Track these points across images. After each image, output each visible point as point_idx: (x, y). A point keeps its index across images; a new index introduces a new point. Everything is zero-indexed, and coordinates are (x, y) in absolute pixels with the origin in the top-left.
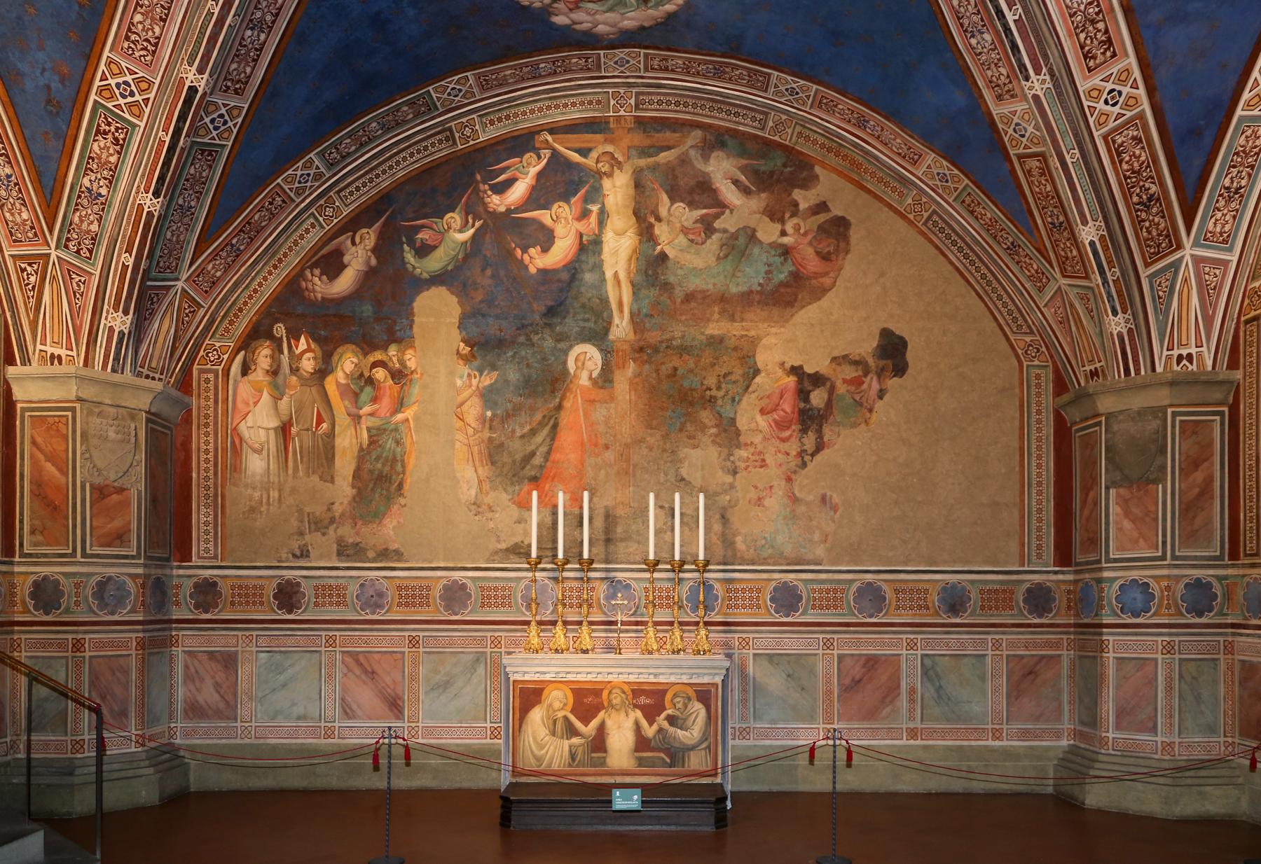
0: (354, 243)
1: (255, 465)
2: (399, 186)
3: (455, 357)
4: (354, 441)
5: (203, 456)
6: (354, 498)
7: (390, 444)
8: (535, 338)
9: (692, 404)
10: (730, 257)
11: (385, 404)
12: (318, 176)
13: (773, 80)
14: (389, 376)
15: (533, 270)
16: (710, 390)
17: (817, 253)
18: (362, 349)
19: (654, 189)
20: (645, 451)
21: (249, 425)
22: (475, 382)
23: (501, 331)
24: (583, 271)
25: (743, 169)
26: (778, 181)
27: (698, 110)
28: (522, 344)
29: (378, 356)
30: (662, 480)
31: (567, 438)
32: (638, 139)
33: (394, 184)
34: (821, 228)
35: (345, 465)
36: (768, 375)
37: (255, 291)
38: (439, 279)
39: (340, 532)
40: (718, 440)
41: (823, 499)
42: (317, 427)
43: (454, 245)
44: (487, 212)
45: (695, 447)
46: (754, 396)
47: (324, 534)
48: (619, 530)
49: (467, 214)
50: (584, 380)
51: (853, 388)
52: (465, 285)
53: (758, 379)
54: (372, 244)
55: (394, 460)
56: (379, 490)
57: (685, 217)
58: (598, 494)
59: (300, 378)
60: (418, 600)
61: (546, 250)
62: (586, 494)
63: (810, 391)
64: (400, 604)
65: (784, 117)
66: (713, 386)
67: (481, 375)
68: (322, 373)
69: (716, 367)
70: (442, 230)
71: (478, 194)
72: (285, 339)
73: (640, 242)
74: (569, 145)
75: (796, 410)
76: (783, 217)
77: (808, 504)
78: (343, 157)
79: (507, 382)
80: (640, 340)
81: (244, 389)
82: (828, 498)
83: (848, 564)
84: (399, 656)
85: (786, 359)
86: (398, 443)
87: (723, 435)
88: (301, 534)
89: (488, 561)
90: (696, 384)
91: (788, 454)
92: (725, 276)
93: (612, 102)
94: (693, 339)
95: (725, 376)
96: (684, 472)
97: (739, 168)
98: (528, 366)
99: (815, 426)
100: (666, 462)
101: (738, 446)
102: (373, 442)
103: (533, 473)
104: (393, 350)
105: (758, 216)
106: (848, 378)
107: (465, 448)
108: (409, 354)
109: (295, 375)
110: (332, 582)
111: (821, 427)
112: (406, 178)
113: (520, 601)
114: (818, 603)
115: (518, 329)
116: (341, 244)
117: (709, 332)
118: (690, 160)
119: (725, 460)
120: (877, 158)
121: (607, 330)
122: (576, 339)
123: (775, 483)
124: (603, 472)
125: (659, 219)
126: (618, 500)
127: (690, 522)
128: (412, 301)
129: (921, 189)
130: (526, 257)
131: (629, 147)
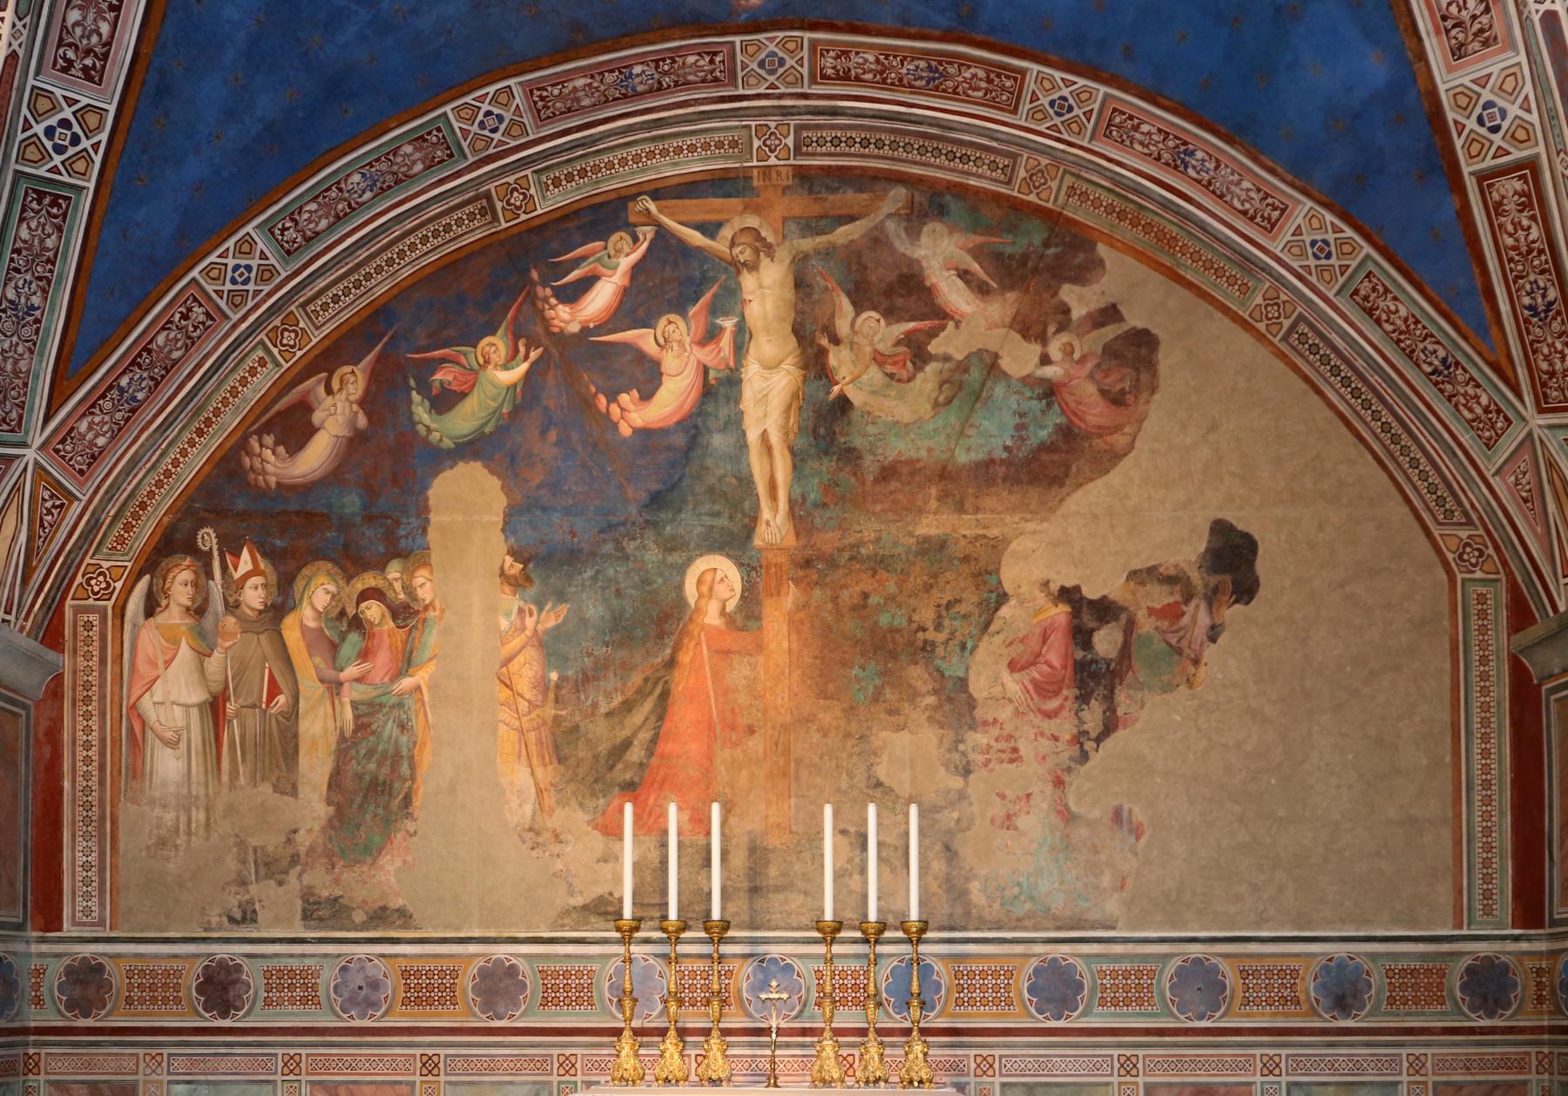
0: (329, 391)
1: (167, 766)
2: (402, 293)
3: (498, 580)
4: (331, 724)
5: (81, 753)
6: (330, 821)
7: (390, 729)
8: (630, 546)
9: (893, 655)
10: (956, 403)
11: (383, 660)
12: (267, 273)
13: (1031, 85)
14: (388, 615)
15: (625, 430)
16: (924, 630)
17: (1104, 393)
18: (343, 569)
19: (826, 288)
20: (816, 737)
21: (156, 699)
22: (530, 622)
23: (574, 535)
24: (710, 432)
25: (976, 253)
26: (1035, 270)
27: (901, 153)
28: (609, 557)
29: (369, 580)
30: (844, 785)
31: (684, 715)
32: (799, 204)
33: (395, 291)
34: (1111, 352)
35: (315, 767)
37: (168, 474)
38: (470, 448)
39: (307, 879)
40: (938, 716)
41: (1117, 815)
42: (269, 702)
43: (495, 391)
44: (550, 334)
45: (900, 728)
46: (998, 639)
47: (281, 883)
48: (773, 871)
49: (516, 338)
50: (712, 617)
51: (1165, 624)
52: (513, 460)
53: (1005, 611)
54: (360, 392)
55: (397, 756)
56: (372, 808)
57: (879, 336)
58: (737, 811)
59: (242, 619)
60: (436, 994)
61: (647, 396)
62: (716, 809)
63: (1093, 630)
64: (406, 1002)
65: (1044, 161)
66: (930, 625)
67: (541, 610)
68: (277, 610)
69: (934, 591)
70: (476, 366)
71: (534, 304)
72: (216, 553)
73: (805, 379)
74: (684, 218)
75: (1070, 662)
76: (1044, 332)
78: (308, 240)
79: (583, 621)
80: (804, 547)
81: (148, 639)
82: (1125, 814)
83: (1160, 926)
84: (405, 1089)
85: (1053, 576)
86: (403, 727)
87: (947, 707)
88: (243, 883)
89: (554, 928)
90: (900, 621)
91: (1056, 739)
92: (948, 436)
93: (756, 143)
94: (895, 544)
95: (949, 606)
96: (881, 772)
97: (970, 251)
98: (618, 593)
99: (1101, 691)
100: (850, 755)
101: (972, 728)
102: (361, 726)
103: (628, 776)
104: (394, 571)
105: (1003, 331)
106: (1158, 606)
107: (514, 735)
108: (421, 576)
109: (233, 614)
110: (294, 963)
111: (1112, 691)
112: (416, 278)
113: (607, 994)
114: (1109, 995)
115: (600, 532)
116: (308, 392)
118: (887, 237)
119: (949, 750)
120: (1203, 226)
121: (749, 531)
122: (699, 546)
123: (1035, 789)
124: (744, 772)
125: (836, 341)
126: (771, 820)
127: (894, 857)
128: (425, 488)
129: (1279, 278)
130: (614, 409)
131: (785, 219)
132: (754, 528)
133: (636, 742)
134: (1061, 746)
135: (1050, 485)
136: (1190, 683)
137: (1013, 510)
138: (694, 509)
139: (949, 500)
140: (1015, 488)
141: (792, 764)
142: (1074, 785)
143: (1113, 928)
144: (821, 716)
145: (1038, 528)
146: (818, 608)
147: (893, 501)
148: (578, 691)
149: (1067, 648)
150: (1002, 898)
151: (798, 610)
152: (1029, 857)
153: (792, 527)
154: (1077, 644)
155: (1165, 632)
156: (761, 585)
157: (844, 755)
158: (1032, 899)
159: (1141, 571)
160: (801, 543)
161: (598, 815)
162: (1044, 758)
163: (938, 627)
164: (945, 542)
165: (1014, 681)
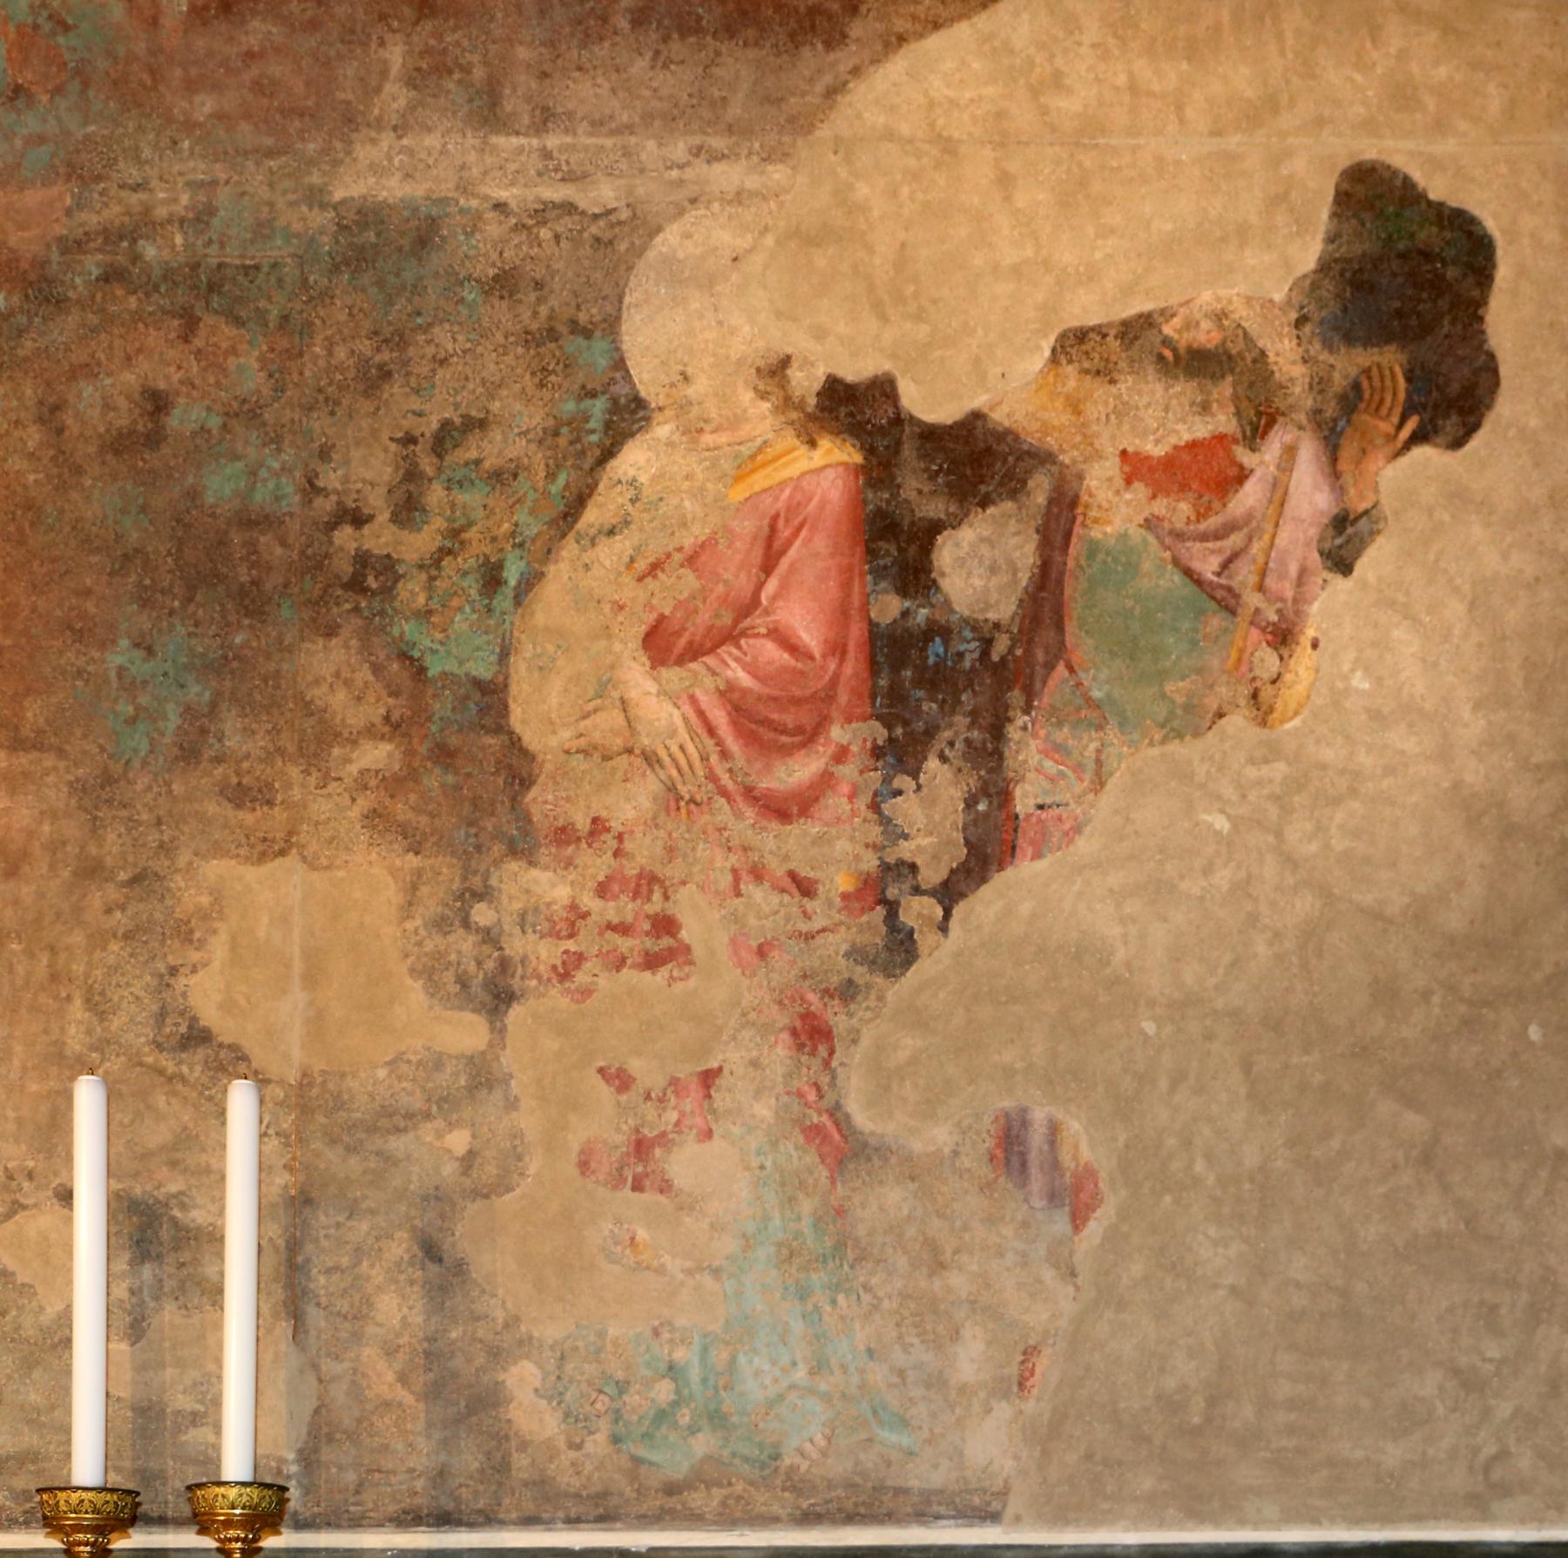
16: (359, 520)
36: (693, 432)
45: (268, 849)
46: (610, 553)
51: (1181, 510)
53: (634, 460)
66: (377, 502)
69: (395, 390)
77: (914, 1171)
82: (1037, 1138)
85: (797, 342)
87: (434, 780)
91: (805, 888)
94: (262, 230)
95: (444, 439)
99: (959, 729)
100: (99, 939)
101: (521, 848)
111: (997, 732)
117: (350, 187)
119: (441, 925)
123: (731, 1057)
134: (821, 912)
135: (796, 40)
136: (1261, 707)
137: (670, 119)
139: (449, 84)
140: (676, 48)
142: (866, 1041)
143: (994, 1517)
145: (753, 182)
147: (257, 86)
149: (846, 586)
150: (617, 1416)
152: (707, 1280)
154: (879, 573)
155: (1179, 536)
157: (78, 938)
158: (717, 1419)
159: (1101, 331)
162: (762, 952)
163: (408, 510)
164: (433, 223)
165: (662, 693)
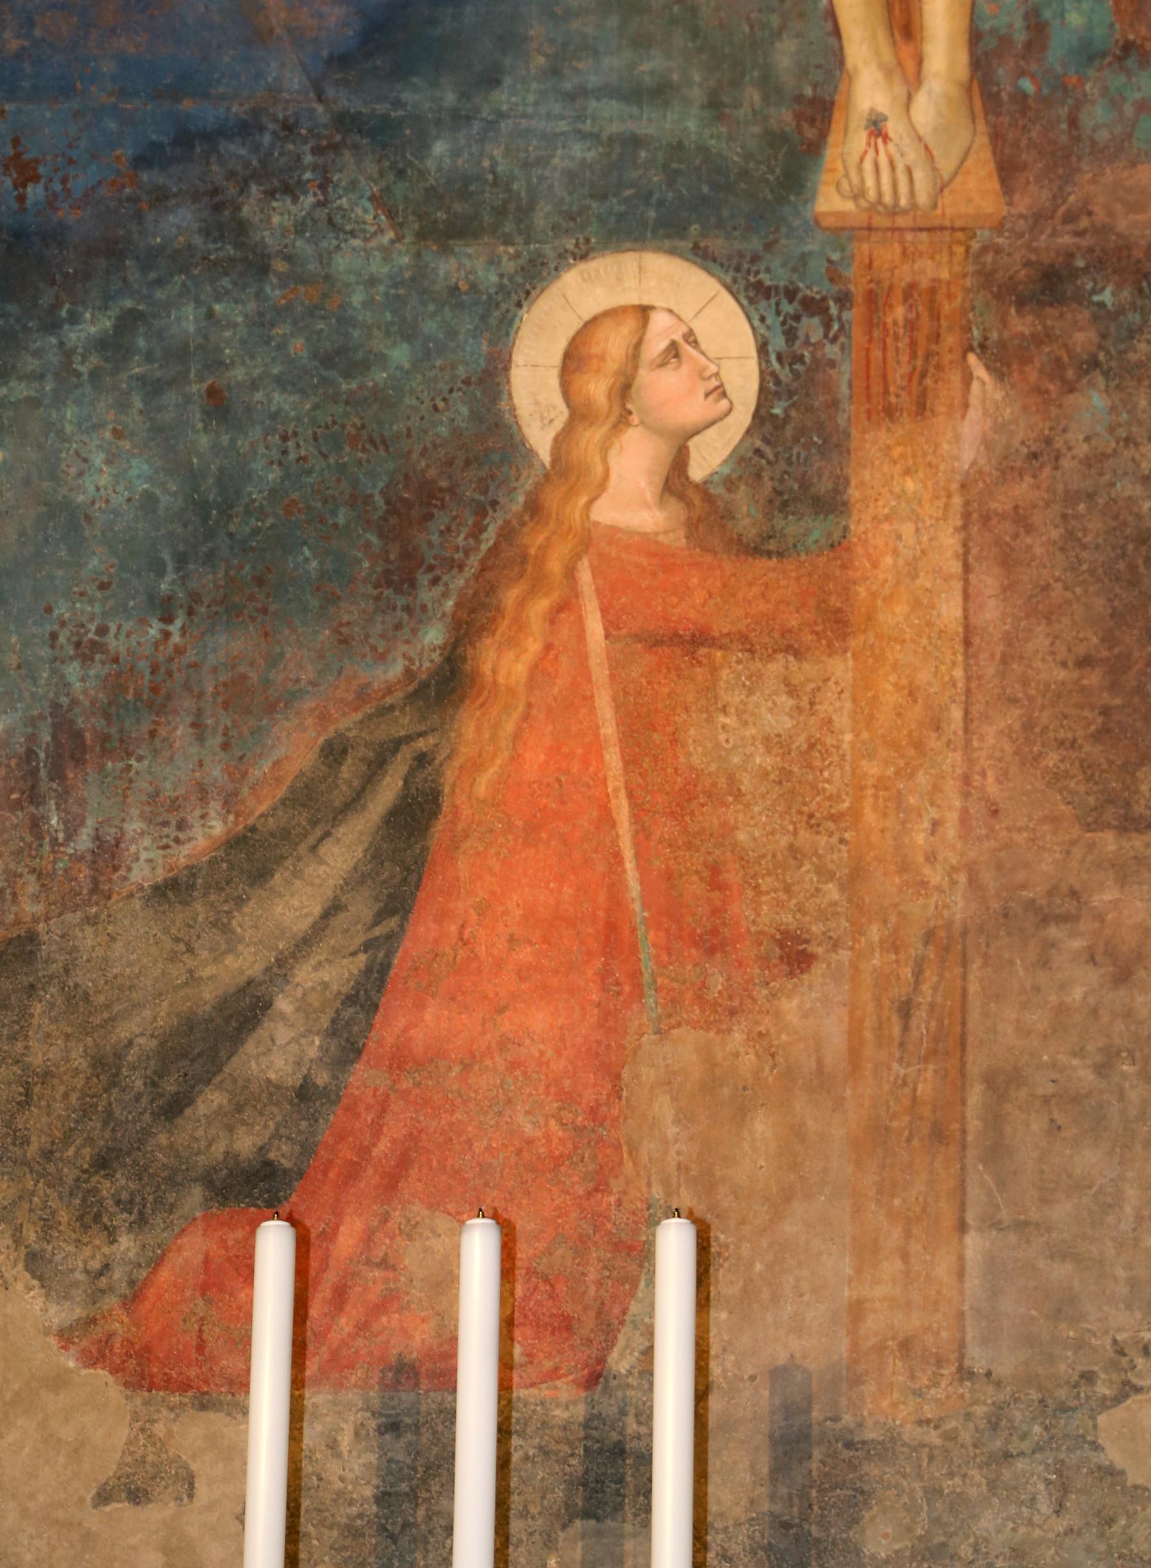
80: (1039, 218)
103: (246, 1143)
115: (142, 161)
122: (573, 219)
124: (762, 1126)
132: (815, 148)
133: (284, 1004)
138: (554, 71)
141: (975, 1095)
144: (1105, 896)
146: (1094, 461)
148: (34, 797)
151: (1007, 472)
153: (983, 140)
156: (844, 376)
160: (1023, 204)
161: (111, 1302)
